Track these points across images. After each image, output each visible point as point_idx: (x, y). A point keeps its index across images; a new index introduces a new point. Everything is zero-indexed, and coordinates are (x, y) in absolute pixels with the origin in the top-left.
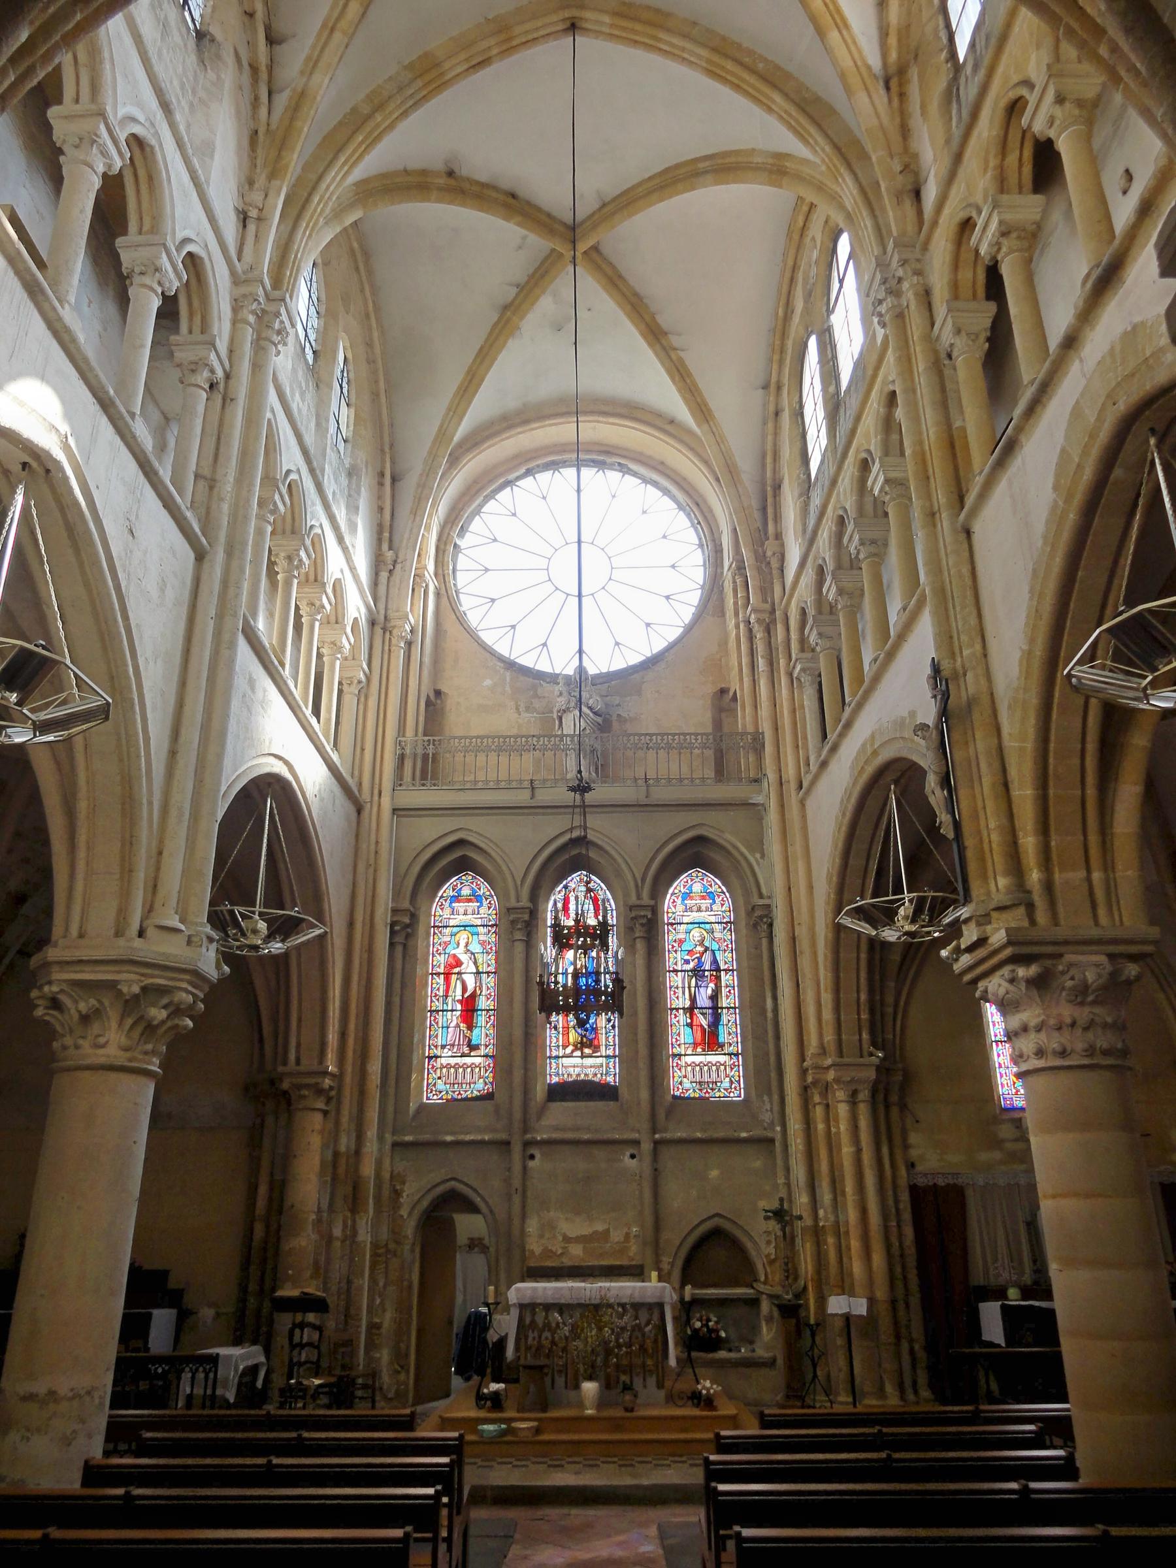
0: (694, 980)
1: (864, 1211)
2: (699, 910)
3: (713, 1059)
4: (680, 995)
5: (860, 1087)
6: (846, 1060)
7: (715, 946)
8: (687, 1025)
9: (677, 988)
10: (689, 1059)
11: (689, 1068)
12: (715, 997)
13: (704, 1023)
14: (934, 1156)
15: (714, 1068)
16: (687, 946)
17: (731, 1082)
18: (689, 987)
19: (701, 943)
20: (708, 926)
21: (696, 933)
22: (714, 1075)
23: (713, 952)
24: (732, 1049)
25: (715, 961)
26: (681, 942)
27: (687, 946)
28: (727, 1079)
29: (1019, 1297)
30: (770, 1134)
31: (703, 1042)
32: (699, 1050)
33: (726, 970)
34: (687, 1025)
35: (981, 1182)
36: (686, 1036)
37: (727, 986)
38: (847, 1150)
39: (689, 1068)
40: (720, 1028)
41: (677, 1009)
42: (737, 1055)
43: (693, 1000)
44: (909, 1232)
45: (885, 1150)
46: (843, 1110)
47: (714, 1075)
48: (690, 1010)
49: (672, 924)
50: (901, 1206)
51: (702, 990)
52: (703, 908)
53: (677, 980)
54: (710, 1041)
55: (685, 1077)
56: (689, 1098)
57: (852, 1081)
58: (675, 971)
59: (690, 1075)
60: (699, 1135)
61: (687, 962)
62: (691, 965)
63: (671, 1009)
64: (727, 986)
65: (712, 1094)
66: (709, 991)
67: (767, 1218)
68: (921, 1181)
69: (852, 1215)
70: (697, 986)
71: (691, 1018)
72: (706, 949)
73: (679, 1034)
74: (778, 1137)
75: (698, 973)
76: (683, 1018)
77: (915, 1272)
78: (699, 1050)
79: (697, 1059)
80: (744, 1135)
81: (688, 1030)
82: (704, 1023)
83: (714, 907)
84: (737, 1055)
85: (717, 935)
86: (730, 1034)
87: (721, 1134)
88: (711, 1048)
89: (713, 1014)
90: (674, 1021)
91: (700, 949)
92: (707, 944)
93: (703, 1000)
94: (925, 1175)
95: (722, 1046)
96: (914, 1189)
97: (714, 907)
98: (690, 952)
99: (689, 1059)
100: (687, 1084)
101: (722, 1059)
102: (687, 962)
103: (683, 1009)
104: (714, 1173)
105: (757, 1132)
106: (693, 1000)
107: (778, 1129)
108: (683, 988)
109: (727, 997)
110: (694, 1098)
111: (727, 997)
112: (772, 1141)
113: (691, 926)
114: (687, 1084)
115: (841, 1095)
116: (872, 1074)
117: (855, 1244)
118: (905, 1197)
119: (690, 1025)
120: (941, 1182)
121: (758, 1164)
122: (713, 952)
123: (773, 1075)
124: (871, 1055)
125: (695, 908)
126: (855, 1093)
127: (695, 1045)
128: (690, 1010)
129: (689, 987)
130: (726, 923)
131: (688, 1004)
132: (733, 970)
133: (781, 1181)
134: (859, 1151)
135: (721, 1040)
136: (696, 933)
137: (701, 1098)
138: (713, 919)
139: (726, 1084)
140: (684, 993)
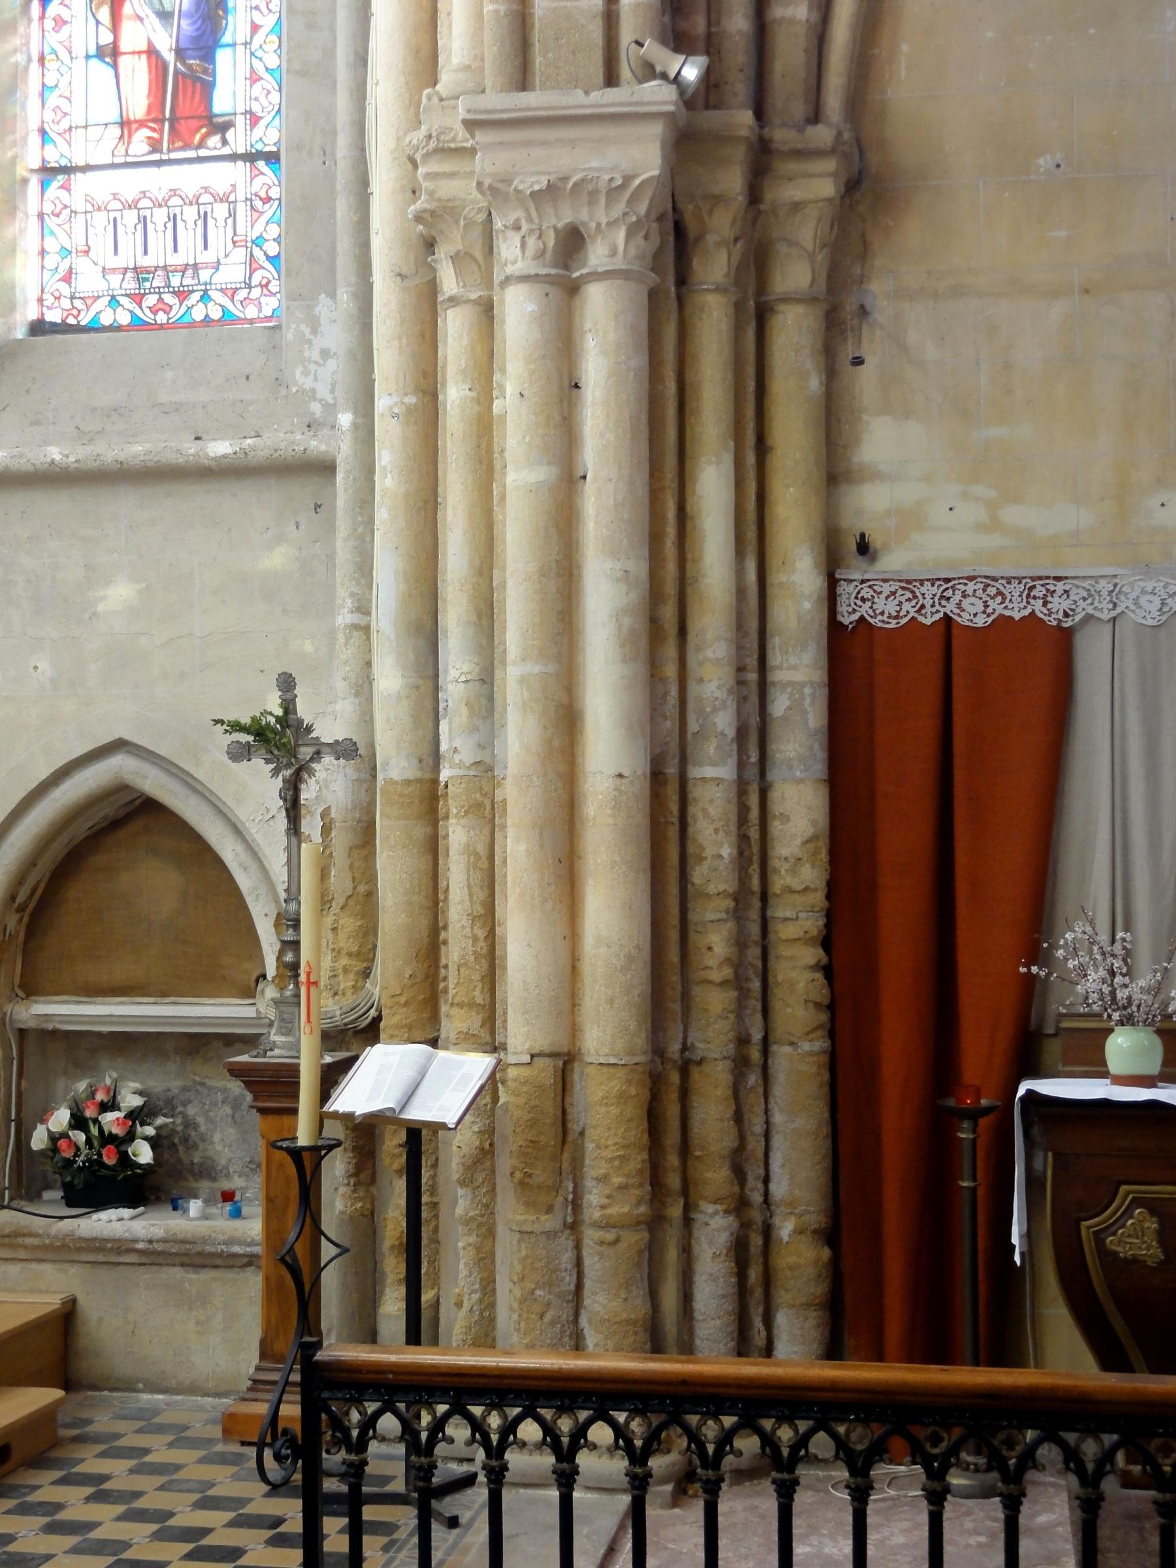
1: (566, 722)
3: (188, 178)
5: (594, 216)
6: (534, 100)
8: (101, 53)
11: (100, 219)
13: (165, 45)
14: (949, 510)
17: (252, 265)
24: (268, 136)
28: (240, 254)
29: (1153, 1064)
30: (317, 445)
31: (155, 117)
32: (139, 145)
34: (101, 53)
35: (1148, 612)
38: (522, 475)
39: (100, 219)
40: (223, 57)
44: (800, 809)
45: (713, 488)
46: (519, 310)
50: (779, 705)
57: (552, 192)
60: (55, 453)
65: (177, 312)
67: (239, 753)
68: (886, 610)
69: (519, 738)
74: (344, 451)
77: (813, 955)
79: (131, 183)
80: (220, 448)
84: (272, 158)
87: (136, 451)
94: (908, 584)
96: (848, 648)
104: (119, 595)
105: (282, 438)
107: (345, 419)
112: (325, 468)
114: (89, 280)
115: (514, 254)
116: (643, 157)
117: (519, 851)
118: (799, 670)
119: (111, 54)
120: (973, 612)
121: (277, 559)
123: (343, 208)
124: (649, 71)
126: (572, 242)
133: (345, 617)
134: (569, 481)
135: (221, 104)
137: (140, 326)
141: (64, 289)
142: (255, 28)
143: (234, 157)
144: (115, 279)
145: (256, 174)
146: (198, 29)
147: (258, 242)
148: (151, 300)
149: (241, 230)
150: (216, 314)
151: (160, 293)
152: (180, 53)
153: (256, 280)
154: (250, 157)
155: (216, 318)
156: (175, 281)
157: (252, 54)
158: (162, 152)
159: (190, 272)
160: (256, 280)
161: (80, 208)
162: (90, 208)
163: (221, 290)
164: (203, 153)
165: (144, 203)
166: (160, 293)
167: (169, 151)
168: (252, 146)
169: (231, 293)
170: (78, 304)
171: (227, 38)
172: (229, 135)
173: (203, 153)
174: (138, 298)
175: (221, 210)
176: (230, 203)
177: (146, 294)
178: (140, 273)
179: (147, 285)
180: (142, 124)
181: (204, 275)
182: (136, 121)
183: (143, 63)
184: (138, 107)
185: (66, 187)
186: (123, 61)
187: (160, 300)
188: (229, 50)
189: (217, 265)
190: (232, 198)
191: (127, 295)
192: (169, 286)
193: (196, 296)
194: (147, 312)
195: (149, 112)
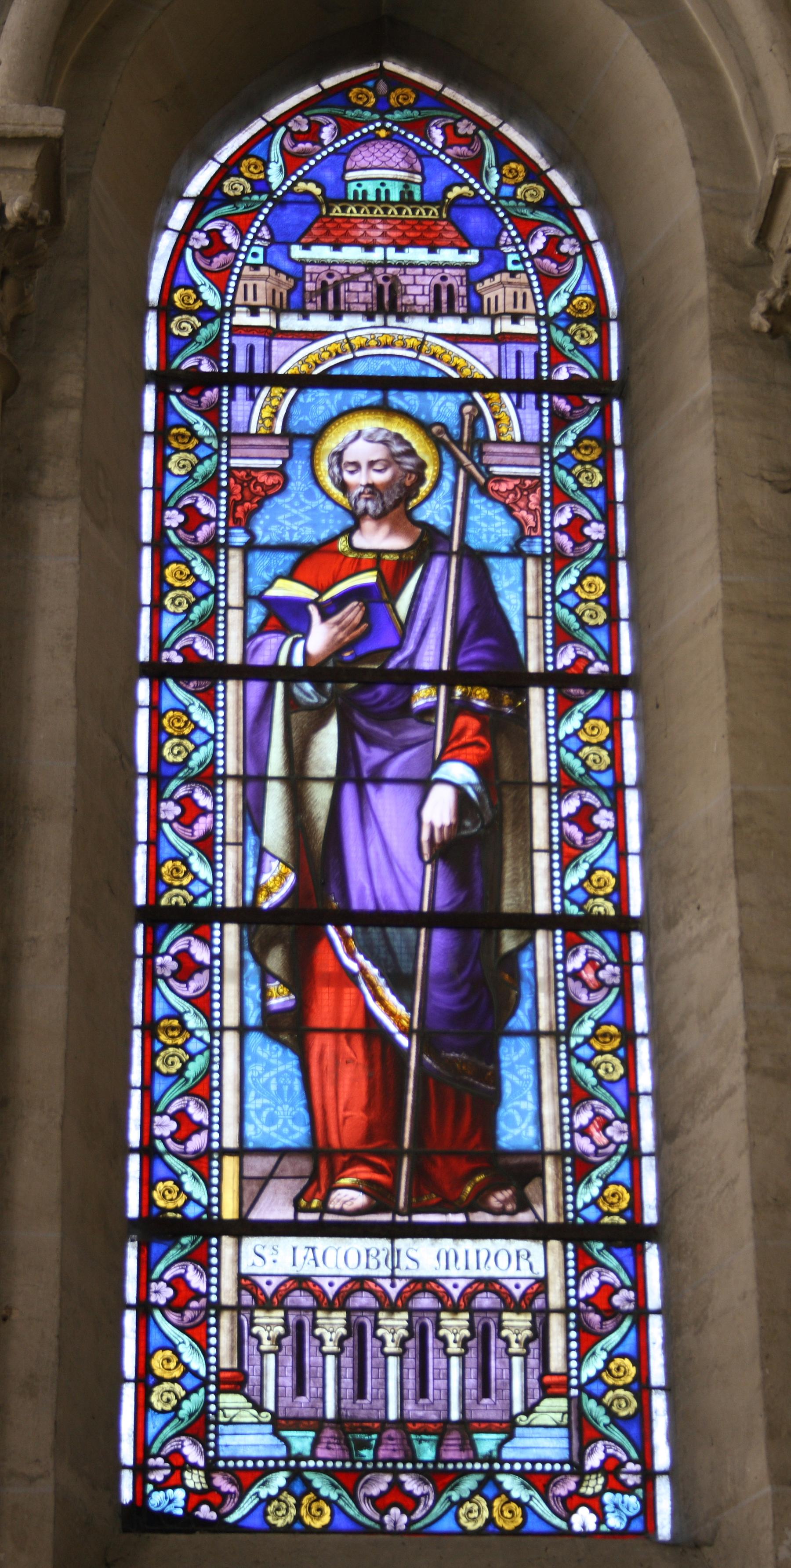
0: (326, 746)
2: (388, 302)
4: (231, 823)
7: (490, 527)
8: (272, 1025)
9: (209, 778)
10: (273, 1259)
11: (269, 1324)
12: (476, 848)
15: (455, 1327)
16: (294, 518)
17: (582, 1431)
18: (297, 779)
19: (397, 500)
20: (444, 407)
21: (361, 442)
22: (454, 1377)
23: (476, 563)
25: (483, 618)
26: (251, 495)
27: (294, 518)
28: (553, 1409)
31: (376, 1149)
32: (348, 1198)
33: (567, 685)
36: (262, 1097)
37: (565, 783)
39: (269, 1324)
40: (513, 1056)
41: (201, 920)
42: (630, 1236)
43: (319, 856)
47: (454, 1377)
48: (290, 931)
49: (194, 384)
51: (389, 804)
52: (417, 291)
53: (220, 726)
54: (428, 1144)
55: (235, 1381)
56: (257, 1531)
58: (204, 675)
59: (271, 1375)
61: (287, 618)
62: (320, 637)
63: (158, 919)
64: (565, 783)
66: (440, 809)
70: (349, 768)
71: (300, 979)
72: (430, 542)
73: (204, 1090)
75: (362, 690)
76: (236, 979)
78: (348, 1198)
79: (337, 1260)
81: (274, 1063)
82: (392, 1012)
83: (495, 292)
85: (508, 467)
86: (576, 1095)
88: (432, 1190)
89: (462, 957)
90: (172, 997)
91: (375, 538)
92: (434, 512)
93: (398, 841)
95: (523, 1170)
97: (495, 292)
98: (307, 558)
99: (273, 1259)
100: (246, 1438)
101: (514, 1262)
102: (287, 618)
103: (246, 916)
106: (319, 856)
108: (254, 781)
109: (568, 853)
110: (297, 1528)
111: (568, 853)
113: (321, 403)
114: (246, 1438)
119: (288, 1029)
122: (476, 563)
125: (360, 291)
127: (320, 1162)
128: (290, 931)
129: (297, 779)
130: (573, 389)
131: (278, 884)
132: (613, 684)
135: (515, 1130)
136: (361, 442)
138: (481, 363)
139: (543, 1441)
140: (253, 815)
141: (192, 1453)
142: (575, 1011)
143: (540, 1232)
144: (301, 1442)
145: (585, 1264)
146: (462, 1001)
147: (597, 1387)
148: (380, 1486)
149: (556, 1364)
150: (509, 1521)
151: (395, 1472)
152: (427, 1037)
153: (594, 1460)
154: (573, 1233)
155: (509, 1526)
156: (427, 1452)
157: (570, 1052)
158: (396, 1211)
159: (453, 1438)
160: (594, 1460)
161: (228, 1297)
162: (247, 1299)
163: (521, 1474)
164: (480, 1217)
165: (363, 1300)
166: (395, 1472)
167: (412, 1209)
168: (576, 1212)
169: (539, 1479)
170: (220, 1482)
171: (521, 1019)
172: (531, 1190)
173: (480, 1217)
174: (348, 1480)
175: (517, 1324)
176: (534, 1313)
177: (365, 1471)
178: (347, 1430)
179: (367, 1454)
180: (355, 1158)
181: (486, 1443)
182: (344, 1152)
183: (355, 1051)
184: (350, 1121)
185: (201, 1258)
186: (320, 1044)
187: (396, 1485)
188: (525, 1044)
189: (508, 1428)
190: (539, 1303)
191: (324, 1470)
192: (415, 1461)
193: (469, 1484)
194: (367, 1508)
195: (369, 1136)
